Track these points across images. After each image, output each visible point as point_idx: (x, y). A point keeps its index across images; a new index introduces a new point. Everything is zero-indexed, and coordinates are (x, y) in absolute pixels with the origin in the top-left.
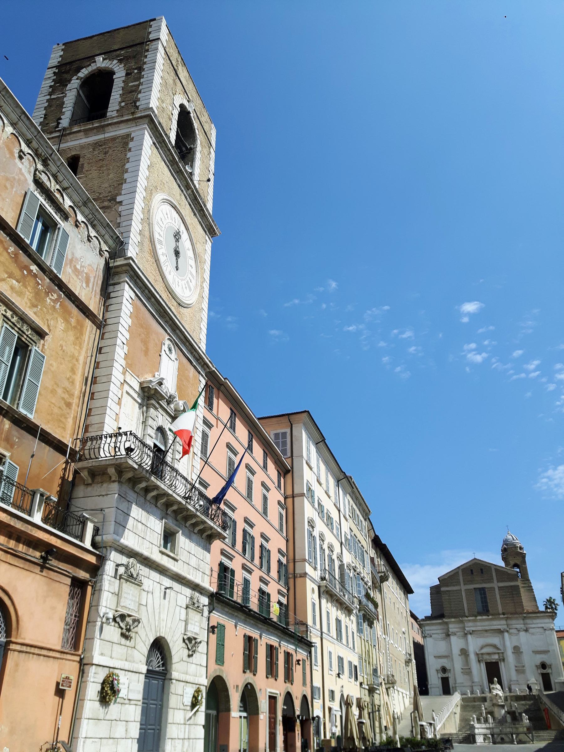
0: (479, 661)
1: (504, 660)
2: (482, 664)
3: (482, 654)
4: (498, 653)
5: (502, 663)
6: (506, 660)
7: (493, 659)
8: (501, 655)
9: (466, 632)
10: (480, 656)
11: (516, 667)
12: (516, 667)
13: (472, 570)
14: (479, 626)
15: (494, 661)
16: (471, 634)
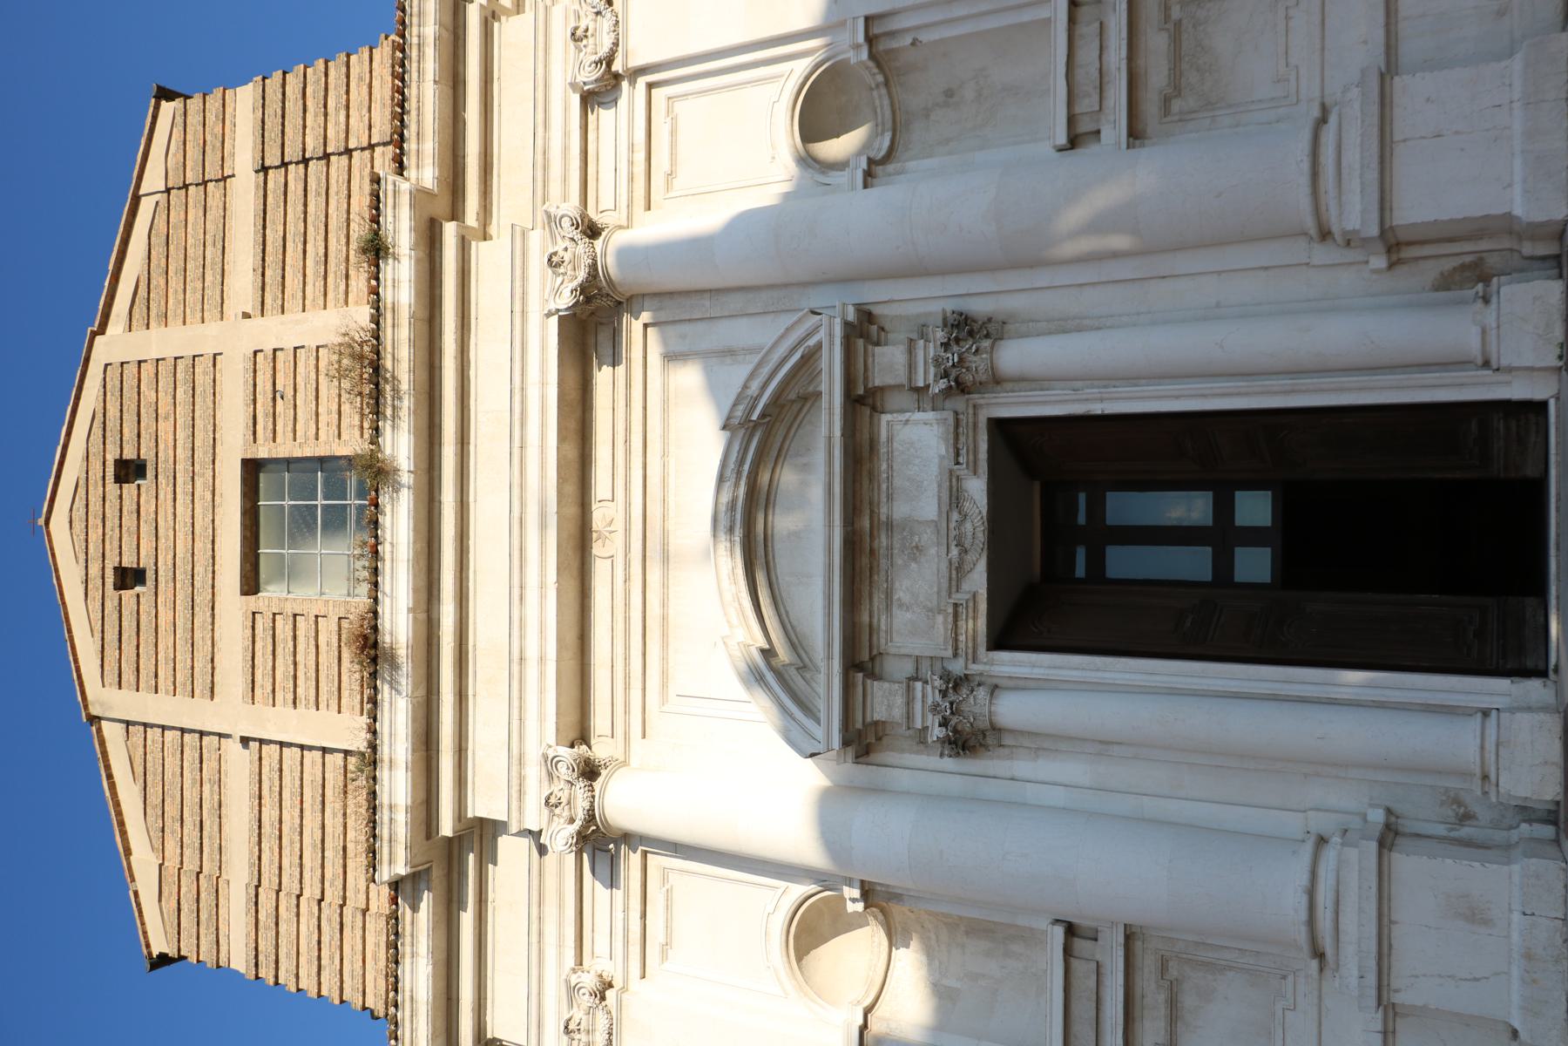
0: (965, 741)
1: (965, 328)
2: (1011, 710)
3: (860, 661)
4: (862, 402)
5: (1013, 356)
6: (979, 307)
7: (955, 498)
8: (888, 363)
9: (561, 836)
10: (884, 701)
11: (1074, 142)
12: (1074, 142)
13: (129, 577)
14: (517, 625)
15: (977, 488)
16: (590, 772)
